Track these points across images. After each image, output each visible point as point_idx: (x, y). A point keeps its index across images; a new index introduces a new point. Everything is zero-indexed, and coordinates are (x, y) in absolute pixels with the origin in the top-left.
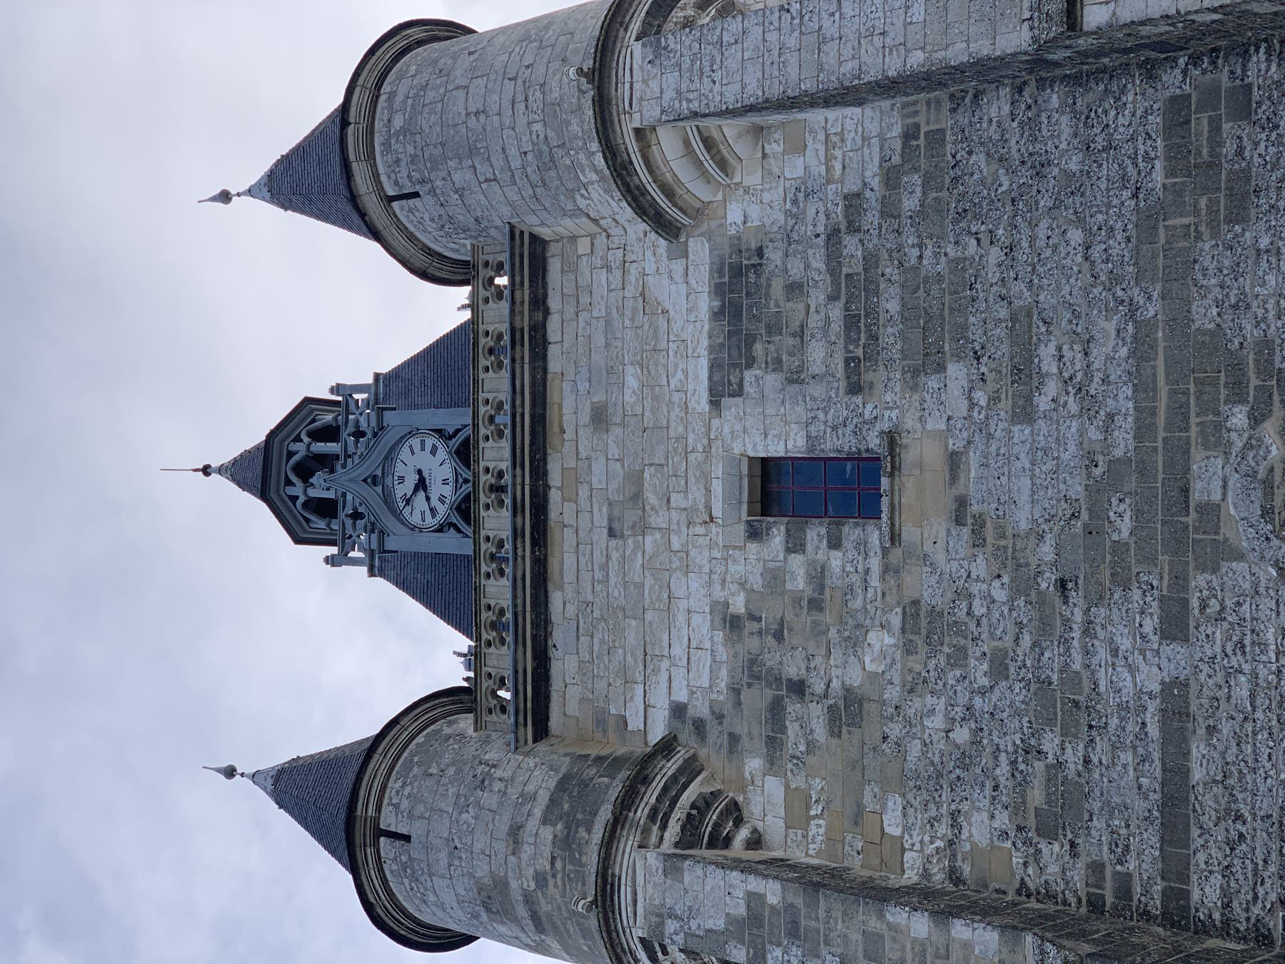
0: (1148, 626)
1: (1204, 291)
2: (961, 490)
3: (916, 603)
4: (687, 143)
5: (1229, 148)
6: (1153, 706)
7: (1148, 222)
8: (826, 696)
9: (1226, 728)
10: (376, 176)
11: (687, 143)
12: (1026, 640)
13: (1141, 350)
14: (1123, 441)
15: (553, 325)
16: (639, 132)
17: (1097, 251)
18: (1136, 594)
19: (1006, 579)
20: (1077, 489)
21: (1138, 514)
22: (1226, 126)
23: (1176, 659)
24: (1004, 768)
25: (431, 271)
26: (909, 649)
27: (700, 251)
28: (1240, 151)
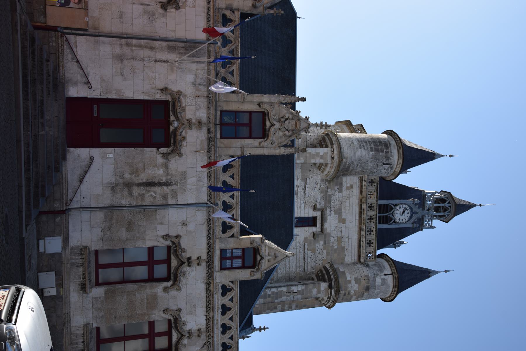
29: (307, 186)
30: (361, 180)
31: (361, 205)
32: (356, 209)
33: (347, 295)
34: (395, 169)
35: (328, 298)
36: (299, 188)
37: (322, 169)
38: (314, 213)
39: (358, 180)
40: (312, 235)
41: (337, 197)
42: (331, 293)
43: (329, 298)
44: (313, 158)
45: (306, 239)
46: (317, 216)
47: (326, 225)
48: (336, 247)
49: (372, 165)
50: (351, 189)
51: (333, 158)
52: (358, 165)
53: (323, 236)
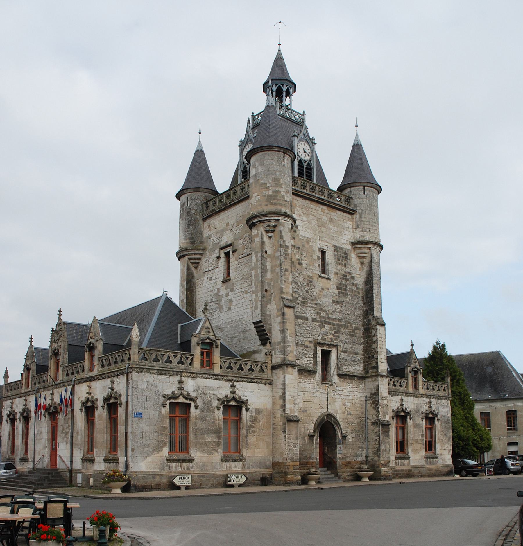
1: (344, 329)
6: (305, 315)
7: (350, 323)
9: (304, 325)
11: (366, 253)
12: (310, 297)
13: (339, 320)
14: (330, 316)
15: (342, 213)
16: (370, 248)
18: (316, 315)
20: (326, 309)
21: (324, 317)
23: (310, 319)
24: (297, 290)
30: (204, 220)
31: (219, 212)
34: (192, 192)
37: (197, 261)
38: (222, 257)
41: (214, 239)
42: (257, 222)
44: (184, 273)
45: (236, 260)
48: (243, 225)
50: (211, 226)
51: (184, 256)
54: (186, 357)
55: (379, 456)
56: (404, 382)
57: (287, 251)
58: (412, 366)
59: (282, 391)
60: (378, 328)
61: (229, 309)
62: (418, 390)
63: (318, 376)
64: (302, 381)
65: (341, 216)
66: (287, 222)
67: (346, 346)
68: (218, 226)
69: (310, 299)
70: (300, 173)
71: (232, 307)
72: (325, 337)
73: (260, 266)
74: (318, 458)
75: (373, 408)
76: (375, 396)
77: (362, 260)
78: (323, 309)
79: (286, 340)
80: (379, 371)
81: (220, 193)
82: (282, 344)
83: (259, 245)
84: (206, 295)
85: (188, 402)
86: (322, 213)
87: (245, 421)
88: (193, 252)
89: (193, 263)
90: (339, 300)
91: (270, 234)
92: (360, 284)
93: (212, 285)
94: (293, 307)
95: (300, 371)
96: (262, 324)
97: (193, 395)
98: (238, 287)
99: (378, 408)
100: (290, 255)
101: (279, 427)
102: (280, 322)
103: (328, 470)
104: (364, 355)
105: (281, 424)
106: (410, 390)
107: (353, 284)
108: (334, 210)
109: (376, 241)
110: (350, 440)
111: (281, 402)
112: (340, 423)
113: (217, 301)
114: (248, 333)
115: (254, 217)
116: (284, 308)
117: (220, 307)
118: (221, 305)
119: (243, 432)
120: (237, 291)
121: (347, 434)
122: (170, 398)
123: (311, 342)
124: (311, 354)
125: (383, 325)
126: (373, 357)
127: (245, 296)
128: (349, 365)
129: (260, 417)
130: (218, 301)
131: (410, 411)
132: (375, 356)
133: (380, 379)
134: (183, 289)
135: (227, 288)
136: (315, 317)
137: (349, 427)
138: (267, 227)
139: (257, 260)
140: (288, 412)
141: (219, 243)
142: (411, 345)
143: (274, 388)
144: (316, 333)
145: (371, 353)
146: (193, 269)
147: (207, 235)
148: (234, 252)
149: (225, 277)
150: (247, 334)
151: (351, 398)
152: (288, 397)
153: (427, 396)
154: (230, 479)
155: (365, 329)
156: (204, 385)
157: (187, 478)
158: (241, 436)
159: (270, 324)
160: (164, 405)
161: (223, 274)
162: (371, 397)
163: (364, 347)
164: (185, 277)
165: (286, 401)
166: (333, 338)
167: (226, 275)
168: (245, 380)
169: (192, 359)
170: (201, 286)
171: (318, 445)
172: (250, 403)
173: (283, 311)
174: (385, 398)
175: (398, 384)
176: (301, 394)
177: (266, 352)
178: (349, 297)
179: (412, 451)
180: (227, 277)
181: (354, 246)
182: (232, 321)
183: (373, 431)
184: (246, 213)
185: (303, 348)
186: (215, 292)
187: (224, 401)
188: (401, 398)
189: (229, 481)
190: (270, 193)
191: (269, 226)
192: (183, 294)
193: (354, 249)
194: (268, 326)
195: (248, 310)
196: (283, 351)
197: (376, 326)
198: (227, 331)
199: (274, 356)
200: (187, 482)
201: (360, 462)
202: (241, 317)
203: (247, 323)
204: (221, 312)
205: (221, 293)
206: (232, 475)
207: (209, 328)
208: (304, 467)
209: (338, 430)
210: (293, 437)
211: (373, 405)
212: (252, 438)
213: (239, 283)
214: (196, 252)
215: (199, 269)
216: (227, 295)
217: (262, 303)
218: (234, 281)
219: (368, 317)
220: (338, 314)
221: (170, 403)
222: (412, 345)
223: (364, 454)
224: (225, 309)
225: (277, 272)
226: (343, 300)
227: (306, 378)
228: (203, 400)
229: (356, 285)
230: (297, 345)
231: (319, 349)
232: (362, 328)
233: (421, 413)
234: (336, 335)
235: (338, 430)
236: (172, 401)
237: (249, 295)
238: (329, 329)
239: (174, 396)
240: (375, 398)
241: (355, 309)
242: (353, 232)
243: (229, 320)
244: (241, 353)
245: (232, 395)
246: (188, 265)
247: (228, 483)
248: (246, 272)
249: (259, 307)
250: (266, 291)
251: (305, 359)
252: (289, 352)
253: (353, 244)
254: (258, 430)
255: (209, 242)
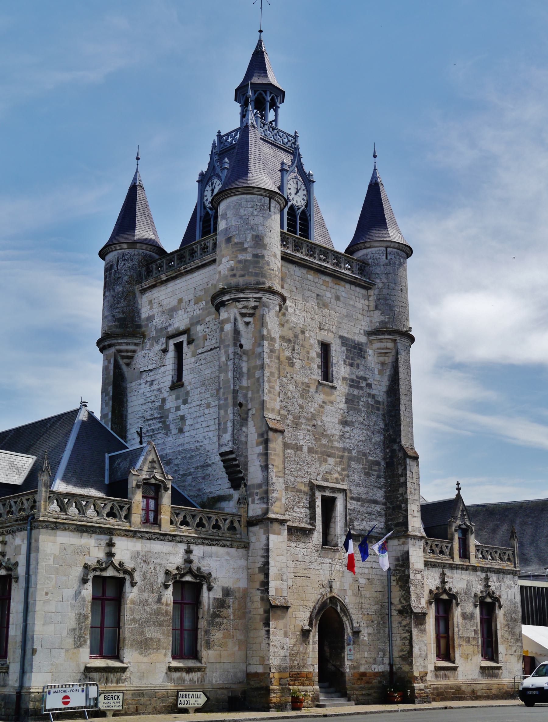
0: (310, 444)
2: (328, 404)
3: (309, 387)
4: (389, 349)
5: (374, 473)
7: (364, 455)
8: (293, 357)
9: (296, 458)
10: (393, 248)
11: (389, 349)
12: (305, 415)
14: (336, 444)
15: (353, 287)
16: (396, 340)
17: (361, 443)
18: (314, 442)
19: (315, 412)
20: (329, 432)
21: (325, 445)
22: (376, 473)
23: (305, 449)
25: (363, 244)
26: (303, 383)
27: (363, 339)
28: (373, 475)
29: (147, 369)
30: (143, 291)
32: (171, 286)
33: (234, 272)
34: (125, 249)
35: (239, 301)
36: (148, 380)
37: (130, 354)
39: (145, 296)
40: (190, 346)
41: (158, 321)
42: (229, 300)
43: (237, 300)
44: (109, 373)
46: (174, 344)
47: (182, 328)
48: (204, 303)
49: (118, 287)
50: (153, 302)
51: (110, 346)
52: (117, 308)
53: (192, 328)
54: (120, 506)
55: (411, 664)
56: (447, 547)
57: (274, 346)
58: (459, 522)
59: (263, 560)
60: (408, 462)
61: (181, 431)
62: (469, 559)
63: (317, 537)
64: (293, 544)
65: (352, 292)
66: (274, 302)
67: (360, 490)
68: (164, 303)
69: (305, 417)
70: (292, 226)
71: (186, 428)
72: (329, 476)
73: (231, 367)
74: (316, 666)
75: (400, 587)
76: (403, 569)
77: (382, 359)
78: (325, 433)
79: (270, 481)
80: (410, 529)
81: (169, 252)
82: (264, 488)
83: (230, 336)
84: (144, 407)
85: (121, 575)
86: (324, 287)
87: (206, 607)
88: (126, 341)
89: (123, 358)
90: (348, 420)
91: (247, 319)
92: (379, 395)
93: (155, 393)
94: (282, 432)
95: (290, 529)
96: (233, 456)
97: (129, 565)
98: (195, 398)
99: (409, 588)
100: (277, 351)
101: (258, 617)
102: (260, 454)
103: (330, 687)
104: (385, 504)
105: (261, 611)
106: (457, 560)
107: (369, 395)
108: (343, 283)
109: (405, 329)
110: (366, 638)
111: (261, 577)
112: (351, 611)
113: (161, 417)
114: (210, 468)
115: (223, 292)
116: (267, 433)
117: (166, 428)
118: (168, 423)
119: (203, 624)
120: (194, 404)
121: (361, 628)
122: (95, 569)
123: (305, 484)
124: (305, 501)
125: (416, 458)
126: (400, 507)
127: (207, 411)
128: (363, 520)
129: (230, 601)
130: (163, 418)
131: (457, 593)
132: (403, 505)
133: (411, 541)
134: (107, 398)
135: (177, 398)
136: (311, 446)
137: (364, 617)
138: (243, 308)
139: (228, 359)
140: (272, 592)
141: (166, 328)
142: (457, 489)
143: (250, 555)
144: (314, 470)
145: (398, 501)
146: (124, 367)
147: (147, 316)
148: (190, 342)
149: (175, 381)
150: (209, 471)
151: (367, 571)
152: (273, 570)
153: (482, 569)
154: (182, 699)
155: (387, 464)
156: (146, 550)
157: (116, 697)
158: (199, 631)
159: (246, 457)
160: (85, 581)
161: (171, 376)
162: (397, 570)
163: (385, 492)
164: (111, 379)
165: (270, 575)
166: (340, 477)
167: (175, 379)
168: (207, 542)
169: (129, 509)
170: (136, 393)
171: (316, 646)
172: (215, 579)
173: (265, 437)
174: (419, 572)
175: (438, 550)
176: (291, 564)
177: (239, 499)
178: (363, 415)
179: (461, 656)
180: (177, 382)
181: (371, 338)
182: (185, 450)
183: (400, 623)
184: (210, 285)
185: (294, 493)
186: (158, 404)
187: (176, 574)
188: (443, 571)
189: (180, 703)
190: (249, 257)
191: (245, 307)
192: (107, 405)
193: (371, 342)
194: (242, 459)
195: (211, 434)
196: (266, 498)
197: (405, 460)
198: (177, 465)
199: (251, 506)
200: (117, 705)
201: (380, 673)
202: (199, 444)
203: (209, 454)
204: (167, 434)
205: (168, 405)
206: (185, 693)
207: (154, 462)
208: (295, 680)
209: (347, 622)
210: (281, 633)
211: (399, 583)
212: (217, 634)
213: (197, 391)
214: (129, 341)
215: (133, 367)
216: (178, 408)
217: (234, 424)
218: (189, 388)
219: (392, 446)
220: (347, 440)
221: (95, 577)
222: (458, 489)
223: (387, 661)
224: (174, 430)
225: (257, 376)
226: (354, 420)
227: (298, 540)
228: (144, 573)
229: (373, 396)
230: (286, 489)
231: (318, 495)
232: (382, 463)
233: (473, 595)
234: (344, 473)
235: (347, 622)
236: (98, 573)
237: (212, 410)
238: (333, 463)
239: (100, 566)
240: (404, 571)
241: (373, 433)
242: (370, 316)
243: (180, 448)
244: (199, 500)
245: (188, 565)
246: (116, 361)
247: (179, 706)
248: (209, 375)
249: (230, 430)
250: (241, 405)
251: (298, 510)
252: (274, 500)
253: (369, 334)
254: (225, 621)
255: (150, 325)
